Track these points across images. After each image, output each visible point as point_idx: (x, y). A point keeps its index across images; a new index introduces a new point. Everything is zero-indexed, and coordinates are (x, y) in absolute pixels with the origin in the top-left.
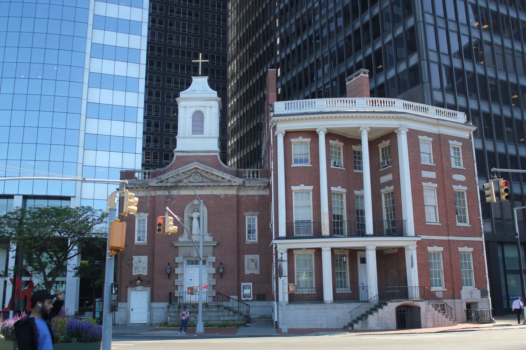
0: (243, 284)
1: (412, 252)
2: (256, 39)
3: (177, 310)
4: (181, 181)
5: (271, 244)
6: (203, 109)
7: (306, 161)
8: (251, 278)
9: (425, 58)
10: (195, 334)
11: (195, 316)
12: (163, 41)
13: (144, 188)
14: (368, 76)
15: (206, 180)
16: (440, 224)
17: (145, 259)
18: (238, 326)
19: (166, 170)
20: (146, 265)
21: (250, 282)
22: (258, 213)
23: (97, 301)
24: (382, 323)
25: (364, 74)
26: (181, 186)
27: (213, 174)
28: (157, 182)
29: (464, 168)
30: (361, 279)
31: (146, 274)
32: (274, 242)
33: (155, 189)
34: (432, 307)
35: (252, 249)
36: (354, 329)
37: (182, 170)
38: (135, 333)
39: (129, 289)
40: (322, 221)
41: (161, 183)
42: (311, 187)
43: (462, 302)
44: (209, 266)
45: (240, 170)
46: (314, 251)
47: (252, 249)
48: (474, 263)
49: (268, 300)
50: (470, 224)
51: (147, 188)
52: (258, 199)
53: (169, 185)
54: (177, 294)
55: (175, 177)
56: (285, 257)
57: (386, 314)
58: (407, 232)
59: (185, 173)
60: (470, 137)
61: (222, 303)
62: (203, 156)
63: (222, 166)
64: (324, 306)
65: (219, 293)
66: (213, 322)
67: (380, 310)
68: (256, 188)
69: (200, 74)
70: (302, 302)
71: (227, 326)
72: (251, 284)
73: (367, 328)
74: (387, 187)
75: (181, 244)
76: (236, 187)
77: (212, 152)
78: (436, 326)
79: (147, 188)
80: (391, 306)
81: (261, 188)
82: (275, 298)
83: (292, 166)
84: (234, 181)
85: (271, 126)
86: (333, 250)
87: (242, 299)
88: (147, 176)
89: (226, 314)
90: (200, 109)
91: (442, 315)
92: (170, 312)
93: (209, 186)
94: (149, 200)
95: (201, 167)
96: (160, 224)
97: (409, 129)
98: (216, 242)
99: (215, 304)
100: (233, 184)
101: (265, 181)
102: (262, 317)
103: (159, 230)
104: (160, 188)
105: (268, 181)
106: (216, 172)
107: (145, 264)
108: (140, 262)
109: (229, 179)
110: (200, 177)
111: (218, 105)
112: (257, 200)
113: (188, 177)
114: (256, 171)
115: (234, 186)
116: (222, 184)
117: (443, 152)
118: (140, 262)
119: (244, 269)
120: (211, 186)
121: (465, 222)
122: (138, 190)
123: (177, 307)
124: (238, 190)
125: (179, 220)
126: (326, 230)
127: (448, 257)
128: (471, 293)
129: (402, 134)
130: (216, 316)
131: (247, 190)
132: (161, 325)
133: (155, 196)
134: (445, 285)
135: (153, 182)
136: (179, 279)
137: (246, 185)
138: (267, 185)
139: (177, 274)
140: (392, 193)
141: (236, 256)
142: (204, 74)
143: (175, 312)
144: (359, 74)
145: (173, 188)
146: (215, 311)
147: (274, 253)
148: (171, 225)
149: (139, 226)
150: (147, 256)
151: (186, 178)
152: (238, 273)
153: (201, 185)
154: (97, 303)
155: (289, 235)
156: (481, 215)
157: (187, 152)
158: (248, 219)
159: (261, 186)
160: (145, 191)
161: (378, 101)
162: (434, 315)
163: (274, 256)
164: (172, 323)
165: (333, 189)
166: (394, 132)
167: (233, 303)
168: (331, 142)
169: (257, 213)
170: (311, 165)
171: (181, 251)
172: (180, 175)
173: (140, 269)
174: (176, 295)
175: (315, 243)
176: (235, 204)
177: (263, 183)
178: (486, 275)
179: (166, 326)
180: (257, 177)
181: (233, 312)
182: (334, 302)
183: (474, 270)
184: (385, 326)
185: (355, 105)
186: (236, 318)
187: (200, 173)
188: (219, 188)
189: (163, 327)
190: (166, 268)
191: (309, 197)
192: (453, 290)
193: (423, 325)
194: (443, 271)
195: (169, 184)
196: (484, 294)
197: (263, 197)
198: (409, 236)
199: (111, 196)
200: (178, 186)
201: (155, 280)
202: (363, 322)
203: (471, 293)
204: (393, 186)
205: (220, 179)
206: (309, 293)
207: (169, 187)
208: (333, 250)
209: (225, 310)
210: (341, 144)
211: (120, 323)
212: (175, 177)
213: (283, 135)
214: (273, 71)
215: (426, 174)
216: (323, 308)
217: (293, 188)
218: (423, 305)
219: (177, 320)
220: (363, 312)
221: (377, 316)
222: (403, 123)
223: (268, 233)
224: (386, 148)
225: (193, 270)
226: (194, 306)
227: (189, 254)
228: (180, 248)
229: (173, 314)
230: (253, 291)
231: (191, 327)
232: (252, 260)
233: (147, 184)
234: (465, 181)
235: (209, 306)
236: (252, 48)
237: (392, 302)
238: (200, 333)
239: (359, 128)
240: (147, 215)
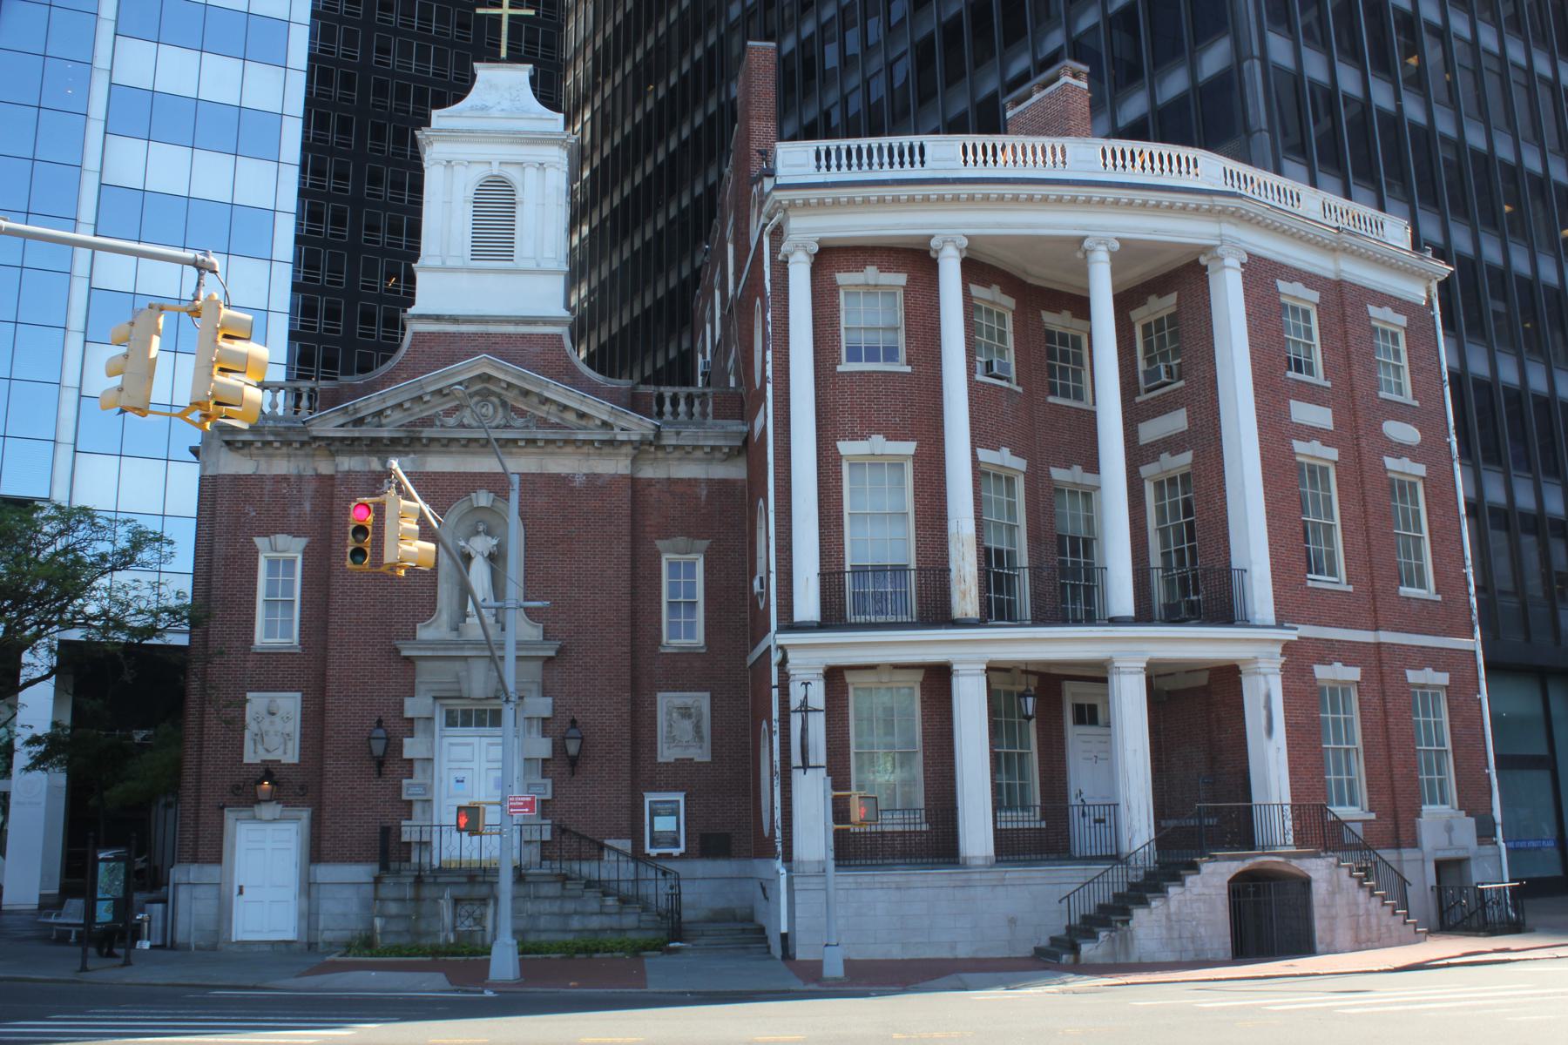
0: (649, 798)
1: (1267, 682)
2: (657, 40)
3: (409, 892)
4: (427, 422)
5: (762, 647)
6: (511, 173)
7: (891, 354)
8: (680, 775)
9: (1256, 52)
10: (488, 986)
11: (478, 912)
12: (361, 12)
13: (295, 445)
14: (1084, 85)
15: (519, 422)
16: (1350, 589)
17: (289, 704)
18: (638, 950)
19: (374, 381)
20: (294, 727)
21: (676, 789)
22: (706, 543)
23: (104, 860)
24: (1180, 937)
25: (1073, 81)
26: (431, 440)
27: (546, 401)
28: (342, 421)
29: (1416, 403)
30: (1081, 779)
31: (296, 760)
32: (776, 638)
33: (333, 448)
34: (1351, 876)
35: (683, 671)
36: (1083, 961)
37: (436, 381)
38: (251, 984)
39: (229, 815)
40: (952, 566)
41: (354, 426)
42: (909, 448)
43: (1423, 861)
44: (529, 732)
45: (643, 389)
46: (918, 676)
47: (683, 671)
48: (1452, 727)
49: (739, 856)
50: (1438, 591)
51: (303, 444)
52: (704, 493)
53: (386, 435)
54: (409, 833)
55: (407, 405)
56: (818, 695)
57: (1195, 905)
58: (1249, 610)
59: (447, 395)
60: (1429, 301)
61: (576, 866)
62: (509, 336)
63: (579, 371)
64: (964, 877)
65: (564, 831)
66: (544, 937)
67: (1173, 891)
68: (699, 454)
69: (504, 53)
70: (880, 862)
71: (597, 951)
72: (680, 797)
73: (1127, 953)
74: (1165, 457)
75: (425, 649)
76: (628, 449)
77: (546, 321)
78: (1364, 946)
79: (303, 444)
80: (1213, 874)
81: (718, 455)
82: (780, 849)
83: (840, 368)
84: (623, 424)
85: (765, 226)
86: (992, 669)
87: (648, 850)
88: (304, 403)
89: (594, 906)
91: (1379, 904)
92: (381, 900)
93: (531, 442)
94: (309, 489)
95: (506, 372)
96: (361, 530)
97: (1250, 255)
98: (557, 644)
99: (549, 871)
100: (620, 437)
101: (735, 428)
102: (721, 917)
103: (359, 553)
104: (350, 445)
105: (745, 429)
106: (557, 392)
108: (273, 714)
109: (605, 418)
110: (500, 410)
111: (566, 162)
112: (703, 498)
113: (457, 408)
114: (698, 397)
115: (623, 443)
116: (581, 437)
117: (1352, 342)
118: (273, 714)
119: (656, 744)
120: (540, 444)
121: (1422, 585)
122: (269, 450)
123: (411, 880)
124: (634, 460)
125: (435, 524)
126: (966, 599)
127: (1376, 700)
128: (1449, 829)
129: (1227, 270)
130: (553, 914)
131: (666, 459)
132: (348, 947)
133: (332, 477)
134: (1370, 800)
135: (329, 425)
136: (419, 777)
137: (664, 442)
138: (739, 443)
139: (411, 761)
140: (1186, 478)
141: (627, 695)
142: (515, 58)
143: (402, 900)
144: (1057, 79)
145: (400, 448)
146: (551, 894)
147: (775, 681)
148: (408, 532)
149: (271, 585)
150: (298, 695)
151: (448, 413)
152: (635, 757)
153: (504, 436)
154: (102, 866)
155: (832, 617)
156: (1469, 562)
157: (454, 319)
158: (671, 564)
159: (719, 448)
160: (296, 455)
161: (1141, 153)
162: (1357, 904)
163: (775, 692)
164: (391, 940)
165: (985, 455)
166: (1197, 261)
167: (613, 867)
168: (976, 290)
169: (706, 543)
170: (908, 369)
171: (427, 675)
172: (427, 398)
173: (273, 741)
174: (405, 838)
175: (928, 646)
176: (626, 507)
177: (726, 436)
178: (1488, 767)
179: (367, 952)
180: (704, 415)
181: (619, 900)
182: (997, 861)
183: (1454, 750)
184: (1190, 947)
185: (1064, 163)
186: (629, 921)
187: (499, 396)
188: (569, 449)
189: (355, 955)
190: (369, 738)
191: (901, 482)
192: (1395, 817)
193: (1321, 943)
194: (1361, 749)
195: (385, 433)
196: (1485, 832)
197: (724, 485)
198: (1258, 623)
199: (132, 324)
200: (419, 439)
201: (329, 782)
202: (1113, 934)
203: (1449, 829)
204: (1191, 452)
205: (571, 417)
206: (907, 828)
207: (385, 441)
208: (992, 669)
209: (589, 894)
210: (1009, 302)
211: (192, 940)
212: (407, 405)
213: (810, 255)
214: (764, 48)
215: (1305, 413)
216: (959, 883)
217: (845, 447)
218: (1320, 870)
219: (408, 931)
220: (1104, 895)
221: (1165, 911)
222: (1230, 230)
223: (742, 616)
224: (1159, 322)
225: (468, 744)
226: (476, 876)
227: (456, 686)
228: (421, 665)
229: (393, 908)
230: (686, 824)
231: (462, 954)
232: (685, 712)
233: (304, 431)
234: (1419, 446)
235: (529, 879)
236: (642, 68)
237: (1214, 859)
238: (505, 984)
239: (1082, 240)
240: (301, 542)
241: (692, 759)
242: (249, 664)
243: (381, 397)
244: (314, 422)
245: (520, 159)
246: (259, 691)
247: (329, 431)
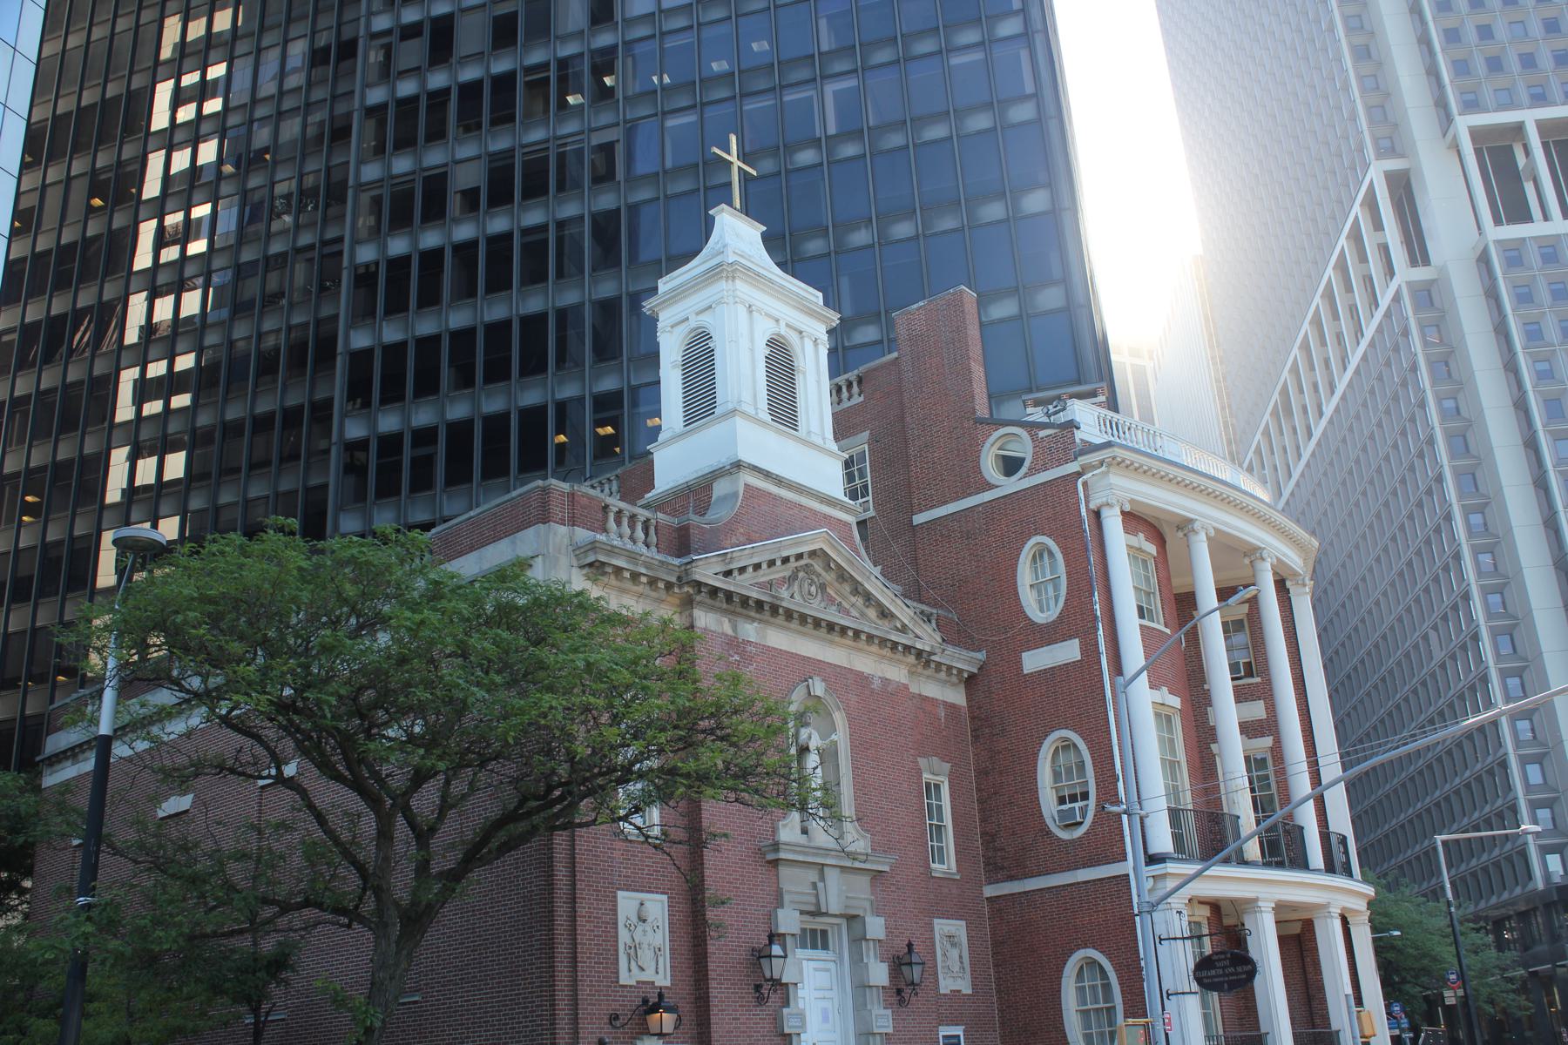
6: (793, 338)
90: (788, 336)
107: (659, 933)
108: (644, 921)
139: (787, 984)
157: (779, 481)
190: (785, 957)
204: (1271, 738)
241: (959, 991)
242: (617, 854)
243: (752, 551)
244: (700, 563)
245: (803, 327)
246: (627, 890)
247: (705, 575)
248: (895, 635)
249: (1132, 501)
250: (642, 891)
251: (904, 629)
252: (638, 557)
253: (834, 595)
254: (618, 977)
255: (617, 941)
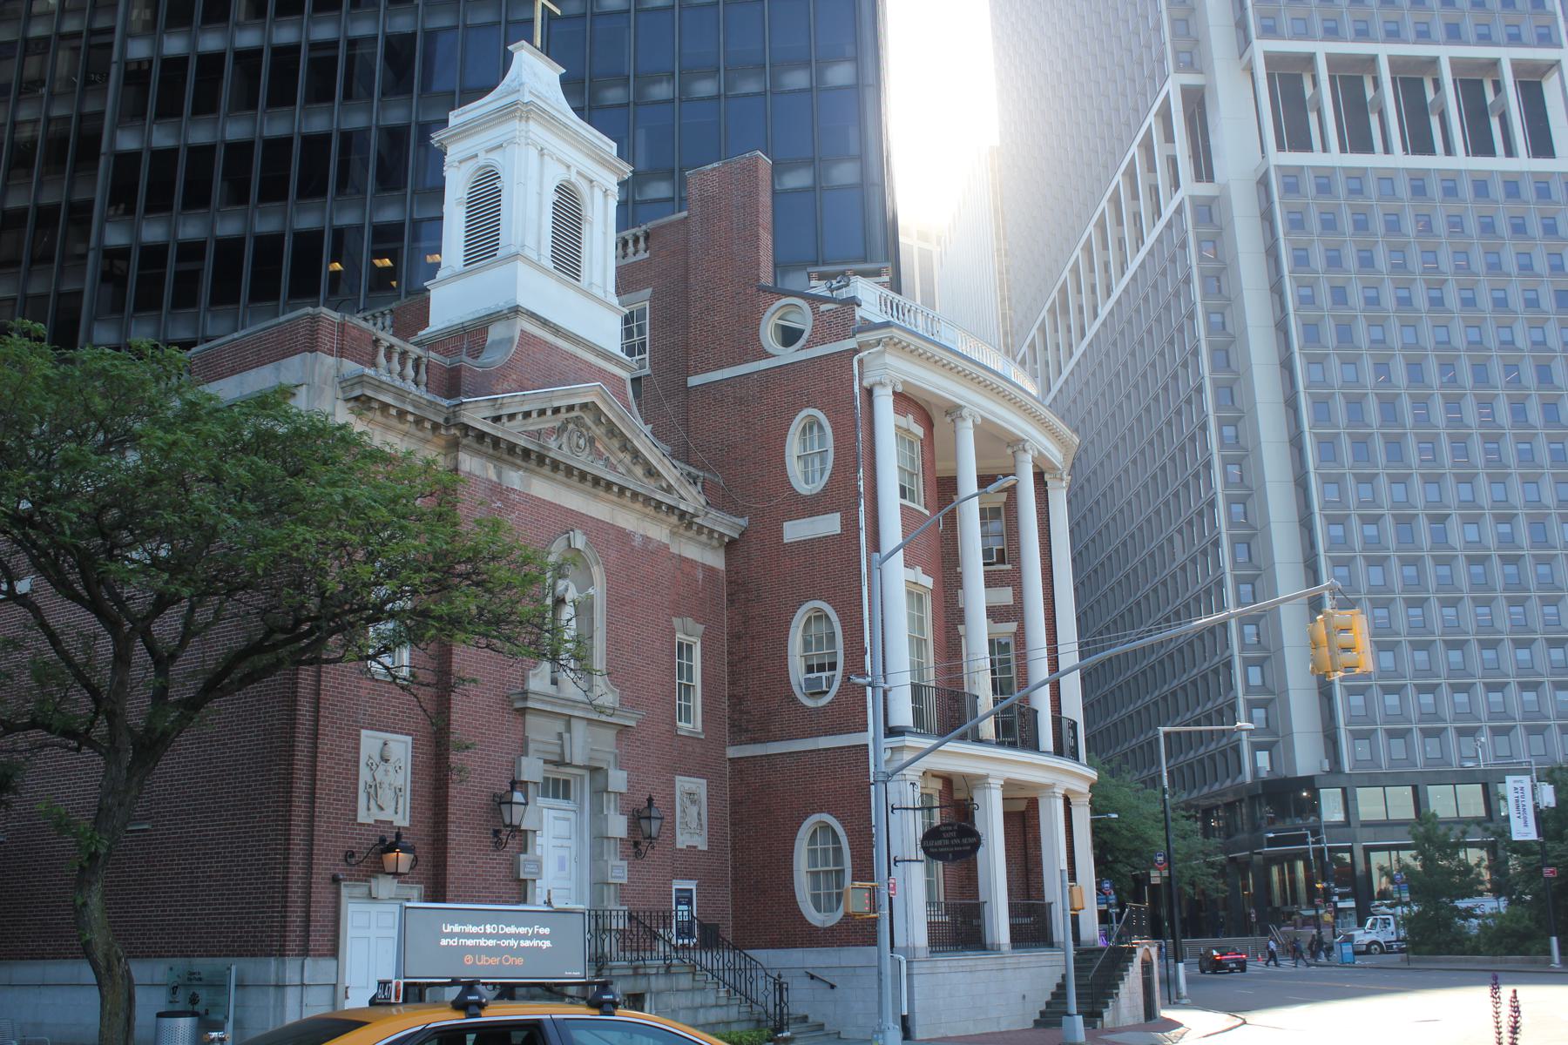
6: (583, 186)
90: (578, 184)
107: (401, 773)
108: (387, 761)
139: (526, 831)
157: (556, 330)
190: (526, 804)
204: (1016, 623)
241: (695, 847)
242: (363, 692)
244: (470, 406)
246: (372, 729)
247: (474, 419)
248: (660, 494)
249: (905, 383)
250: (387, 731)
251: (669, 489)
252: (406, 395)
253: (602, 449)
254: (356, 815)
255: (357, 779)
